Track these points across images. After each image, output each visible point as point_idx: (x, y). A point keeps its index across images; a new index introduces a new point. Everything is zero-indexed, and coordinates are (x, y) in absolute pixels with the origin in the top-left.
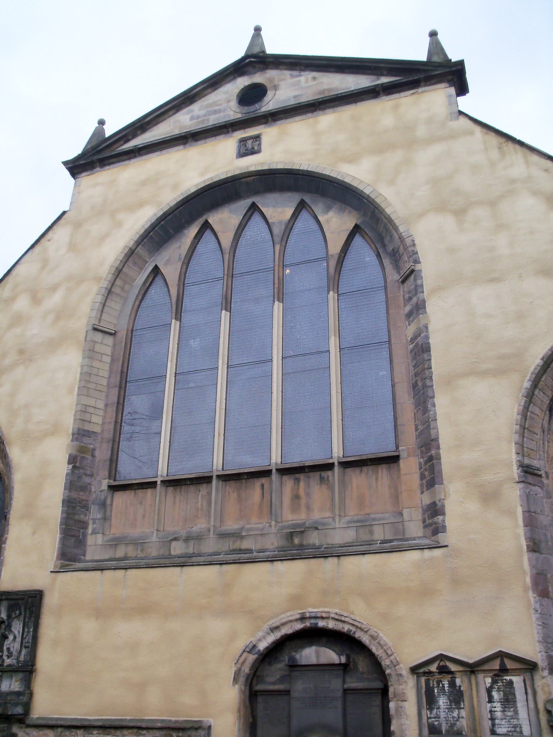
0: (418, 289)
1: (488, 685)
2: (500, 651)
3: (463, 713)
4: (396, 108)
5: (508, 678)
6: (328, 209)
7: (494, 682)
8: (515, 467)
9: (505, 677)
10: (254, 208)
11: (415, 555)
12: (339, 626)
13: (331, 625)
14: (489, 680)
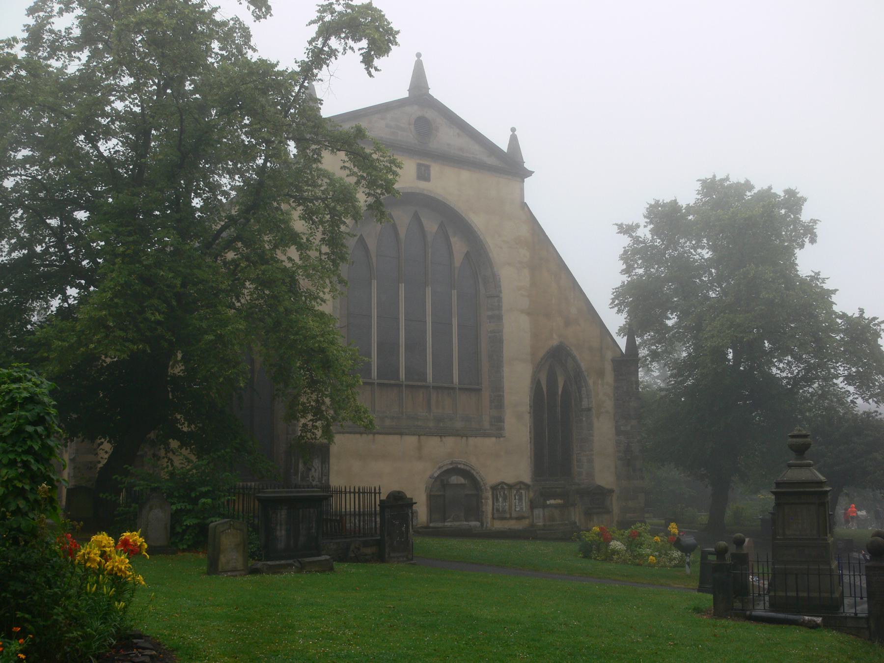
0: (499, 308)
8: (528, 406)
11: (494, 439)
12: (465, 467)
13: (462, 467)
14: (515, 492)
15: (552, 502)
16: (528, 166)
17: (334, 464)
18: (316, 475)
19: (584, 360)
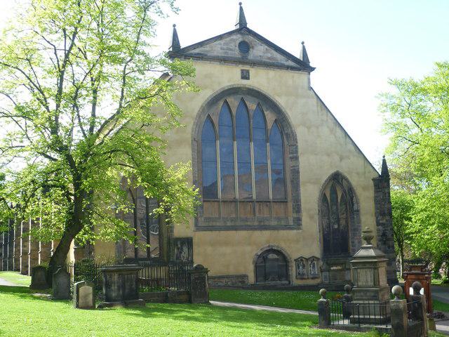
0: (297, 152)
4: (293, 77)
6: (267, 109)
10: (242, 100)
11: (295, 231)
15: (334, 268)
16: (311, 65)
17: (196, 249)
18: (186, 255)
19: (354, 181)
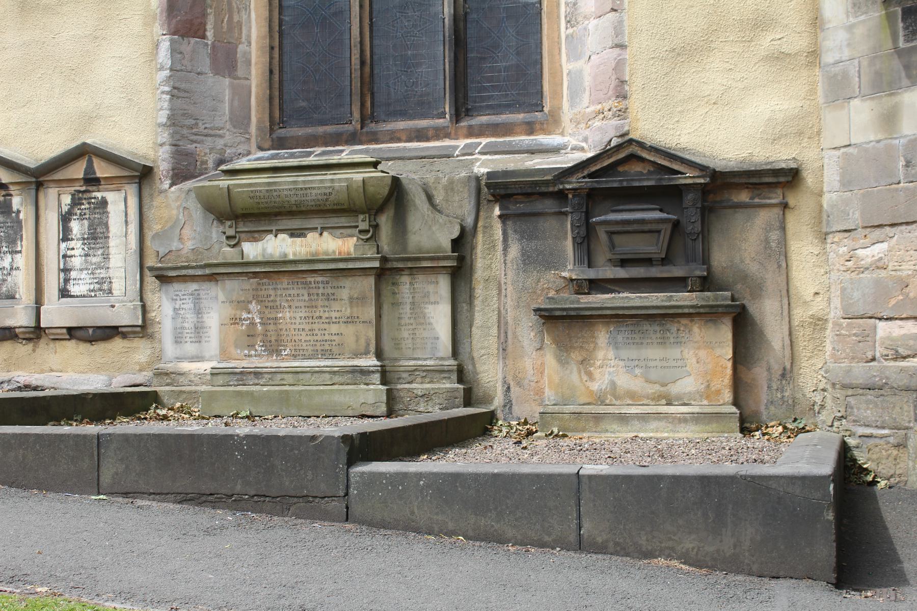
1: (65, 209)
2: (84, 144)
3: (20, 260)
5: (99, 195)
7: (76, 202)
9: (94, 194)
14: (67, 200)
